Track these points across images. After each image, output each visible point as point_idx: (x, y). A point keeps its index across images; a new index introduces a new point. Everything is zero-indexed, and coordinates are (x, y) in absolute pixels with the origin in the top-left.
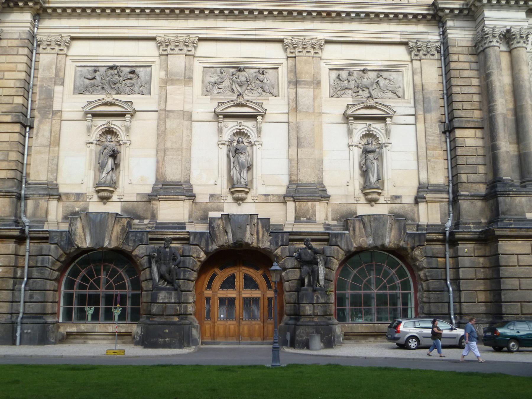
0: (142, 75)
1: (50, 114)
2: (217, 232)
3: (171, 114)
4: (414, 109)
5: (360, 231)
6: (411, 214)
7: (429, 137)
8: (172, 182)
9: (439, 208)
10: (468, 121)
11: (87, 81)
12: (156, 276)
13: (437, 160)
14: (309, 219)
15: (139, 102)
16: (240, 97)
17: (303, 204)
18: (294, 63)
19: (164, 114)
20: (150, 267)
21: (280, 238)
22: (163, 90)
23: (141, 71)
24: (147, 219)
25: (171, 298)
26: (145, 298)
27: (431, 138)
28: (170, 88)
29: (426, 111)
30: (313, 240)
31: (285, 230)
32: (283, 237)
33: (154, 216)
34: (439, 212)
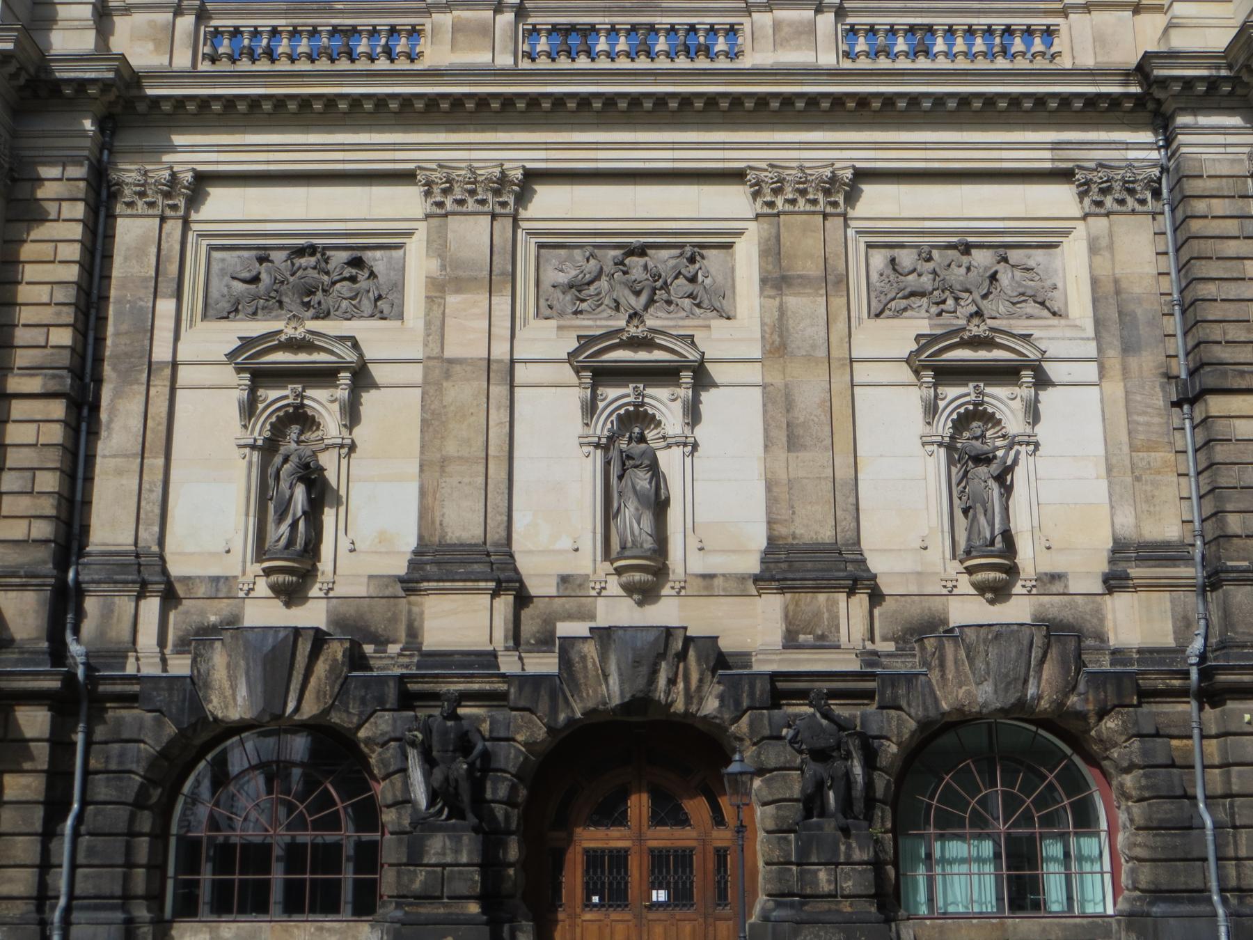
0: (379, 268)
1: (141, 371)
2: (580, 676)
3: (457, 368)
4: (1094, 344)
5: (957, 669)
6: (1095, 621)
7: (1136, 418)
8: (461, 545)
9: (1168, 604)
10: (1242, 373)
11: (239, 287)
12: (420, 795)
13: (1159, 477)
14: (822, 637)
15: (375, 339)
16: (635, 322)
17: (805, 598)
18: (774, 231)
19: (440, 368)
20: (404, 770)
21: (746, 688)
22: (435, 307)
23: (377, 260)
24: (394, 642)
25: (457, 851)
26: (391, 850)
27: (1141, 419)
28: (453, 300)
29: (1128, 348)
30: (834, 694)
31: (758, 668)
32: (752, 687)
33: (413, 633)
34: (1169, 614)
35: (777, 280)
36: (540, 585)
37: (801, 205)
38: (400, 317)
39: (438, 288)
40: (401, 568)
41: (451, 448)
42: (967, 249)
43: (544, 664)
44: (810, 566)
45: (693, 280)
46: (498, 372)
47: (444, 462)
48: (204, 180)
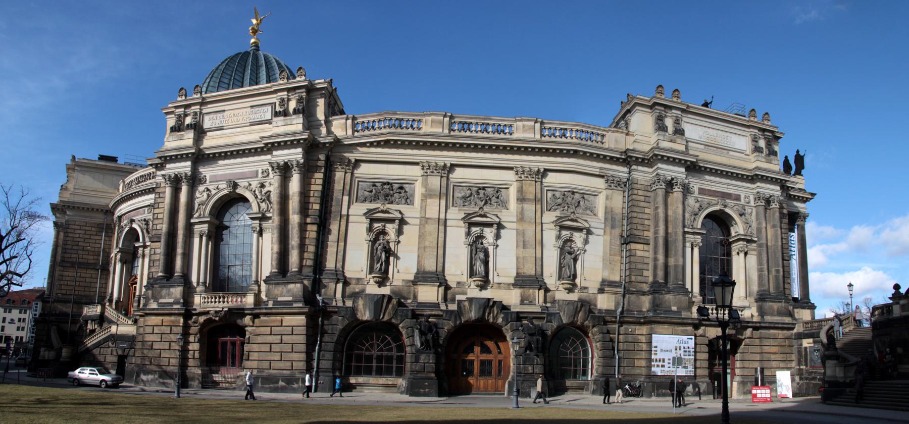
0: (407, 190)
11: (367, 193)
12: (418, 343)
17: (527, 290)
19: (425, 220)
20: (413, 336)
23: (407, 187)
26: (408, 358)
28: (429, 201)
30: (534, 318)
31: (512, 310)
33: (415, 297)
35: (521, 199)
36: (452, 284)
37: (529, 178)
38: (413, 204)
39: (425, 197)
40: (412, 278)
41: (427, 244)
42: (573, 193)
43: (453, 307)
44: (528, 281)
45: (498, 198)
46: (442, 222)
47: (425, 248)
48: (358, 162)
